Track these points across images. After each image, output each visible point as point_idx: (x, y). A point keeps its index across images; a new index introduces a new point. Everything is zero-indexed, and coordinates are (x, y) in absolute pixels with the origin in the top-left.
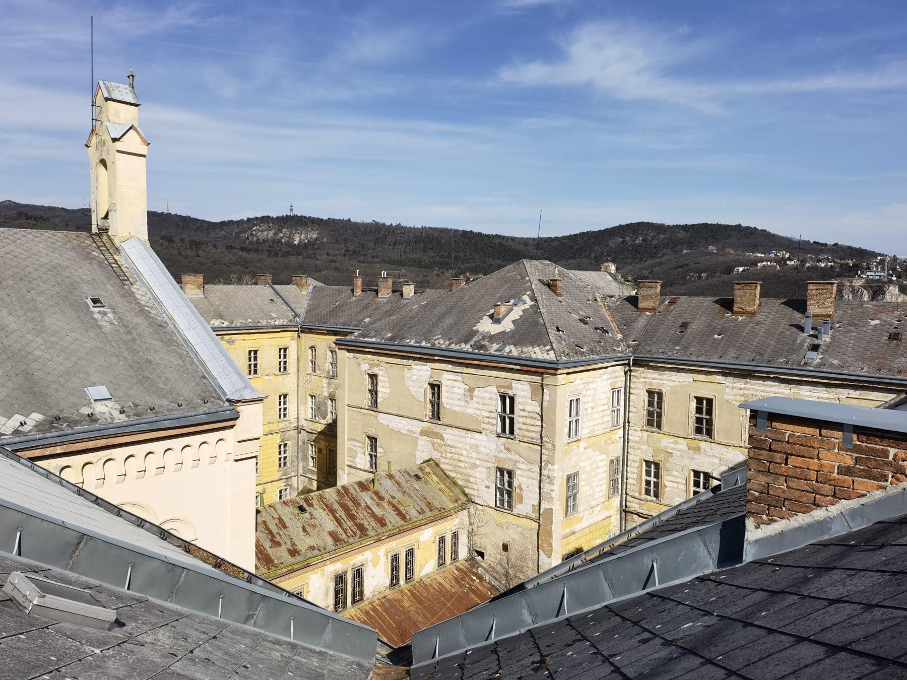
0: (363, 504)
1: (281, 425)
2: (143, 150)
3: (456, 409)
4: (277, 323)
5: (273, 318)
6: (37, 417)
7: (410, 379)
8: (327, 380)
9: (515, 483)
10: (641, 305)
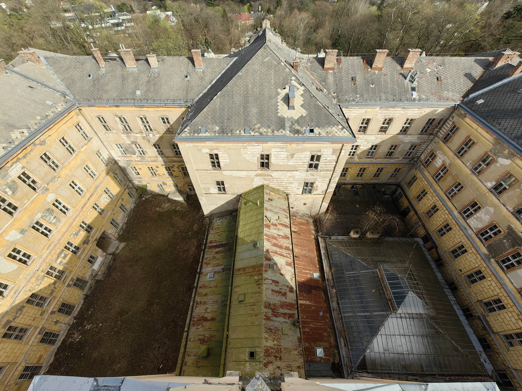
0: (277, 236)
3: (281, 163)
4: (59, 109)
5: (51, 107)
7: (246, 153)
8: (126, 135)
9: (315, 185)
10: (326, 66)
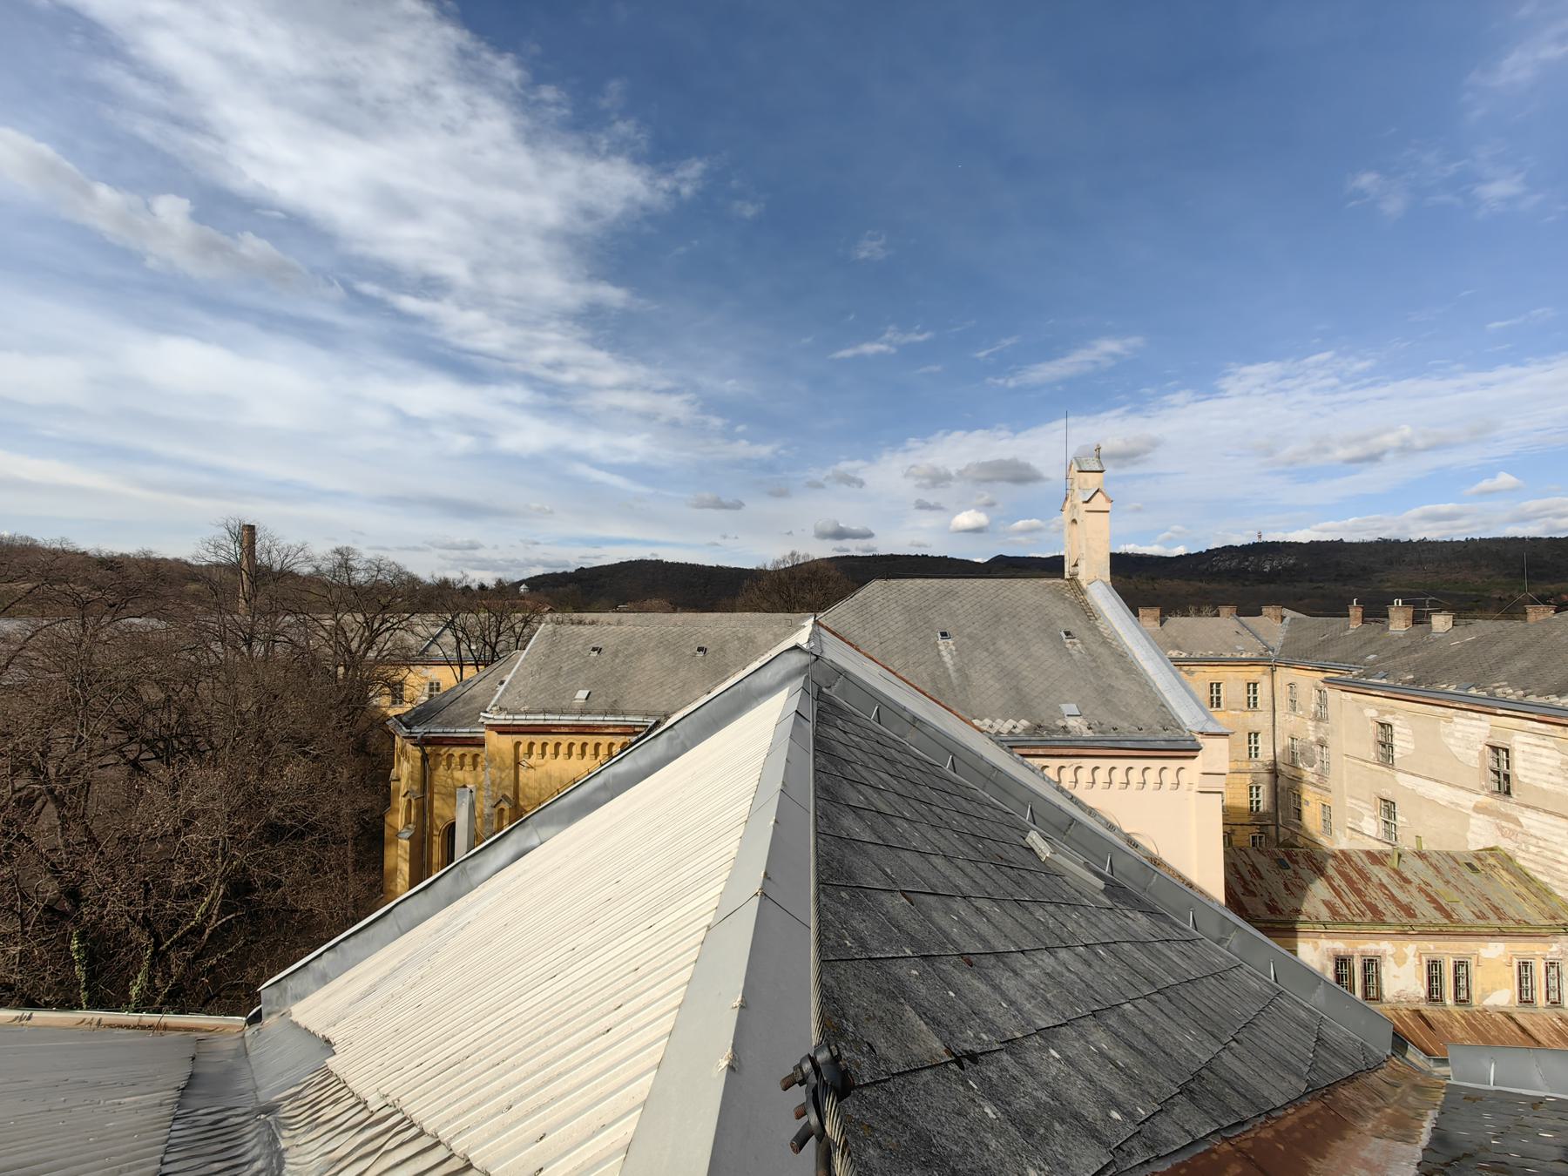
0: (1374, 880)
1: (1252, 766)
2: (1107, 507)
3: (1545, 786)
6: (1024, 723)
